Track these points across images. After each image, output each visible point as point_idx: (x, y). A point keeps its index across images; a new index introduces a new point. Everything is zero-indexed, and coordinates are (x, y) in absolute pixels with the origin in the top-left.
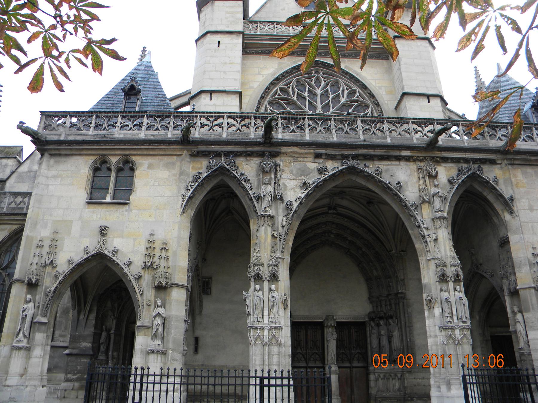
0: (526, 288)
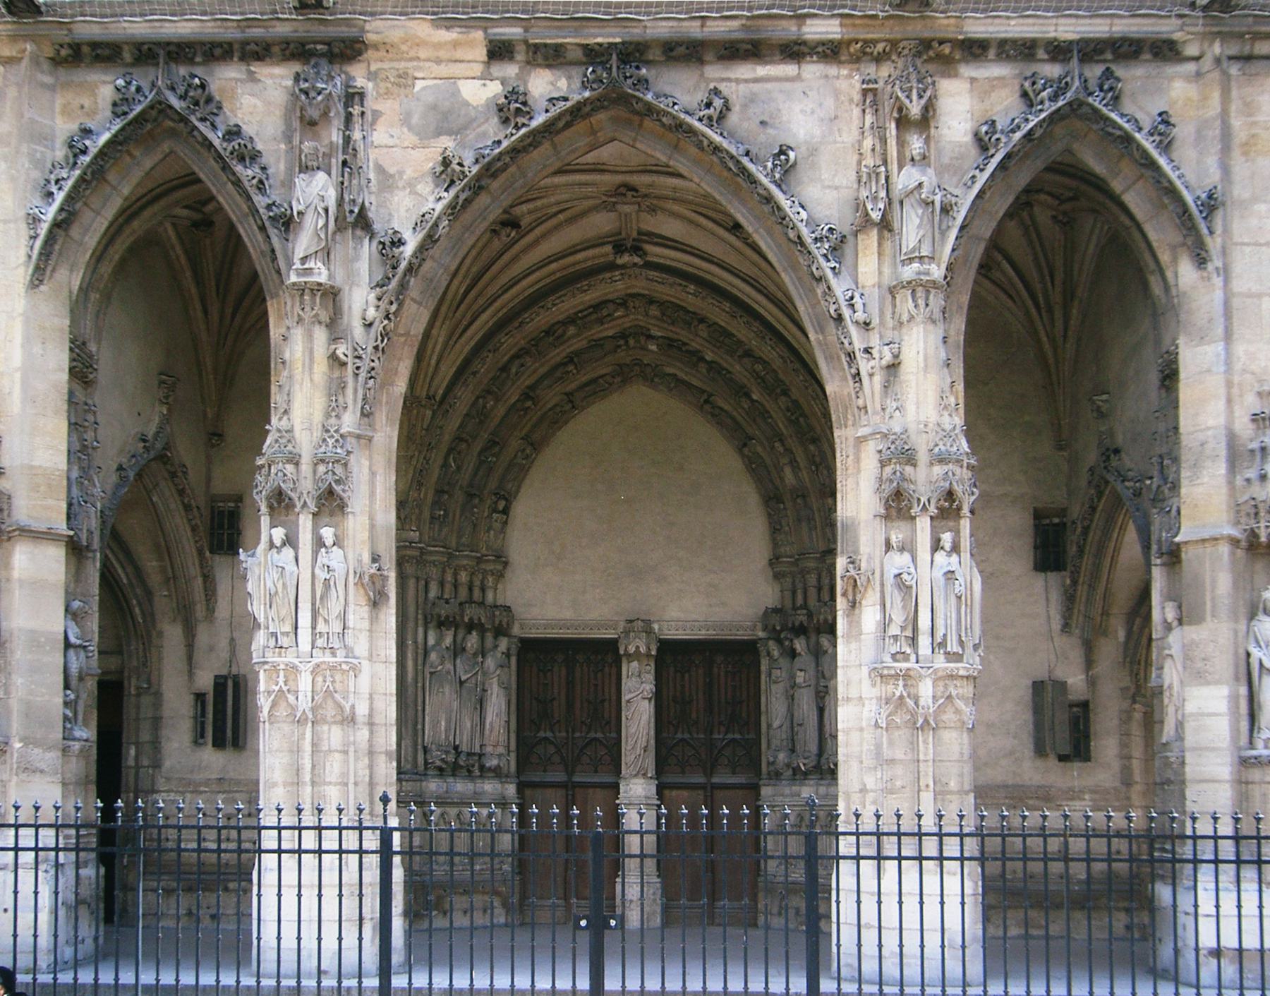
0: (1204, 541)
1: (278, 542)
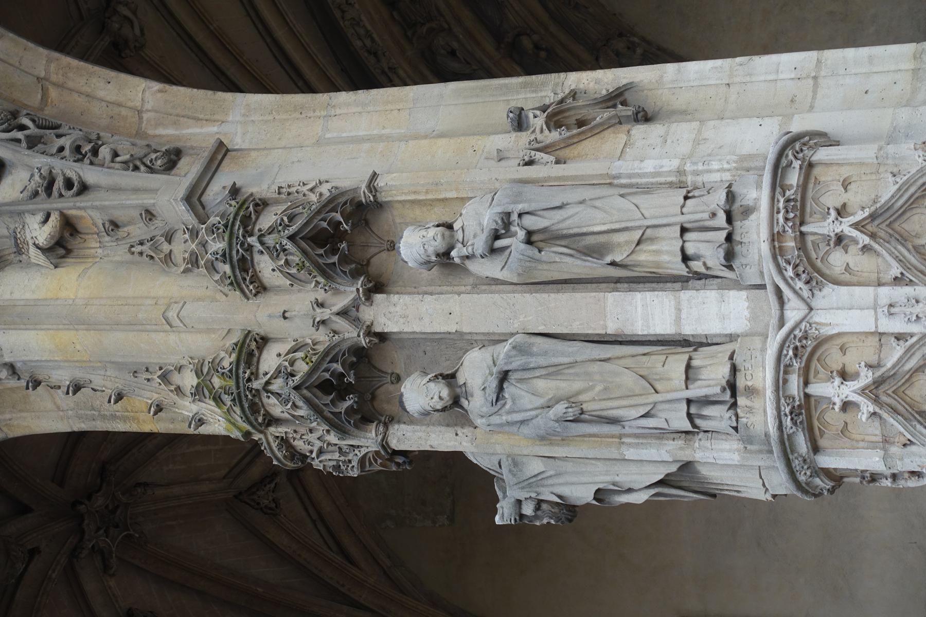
1: (440, 392)
